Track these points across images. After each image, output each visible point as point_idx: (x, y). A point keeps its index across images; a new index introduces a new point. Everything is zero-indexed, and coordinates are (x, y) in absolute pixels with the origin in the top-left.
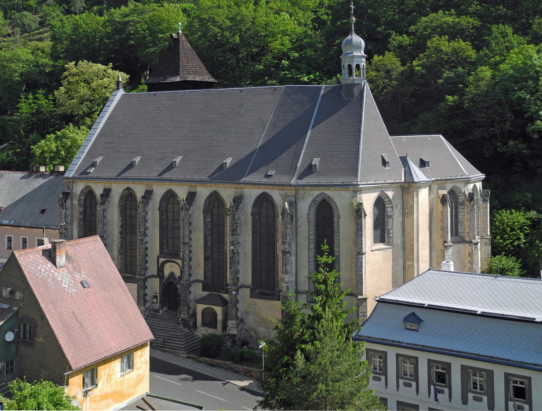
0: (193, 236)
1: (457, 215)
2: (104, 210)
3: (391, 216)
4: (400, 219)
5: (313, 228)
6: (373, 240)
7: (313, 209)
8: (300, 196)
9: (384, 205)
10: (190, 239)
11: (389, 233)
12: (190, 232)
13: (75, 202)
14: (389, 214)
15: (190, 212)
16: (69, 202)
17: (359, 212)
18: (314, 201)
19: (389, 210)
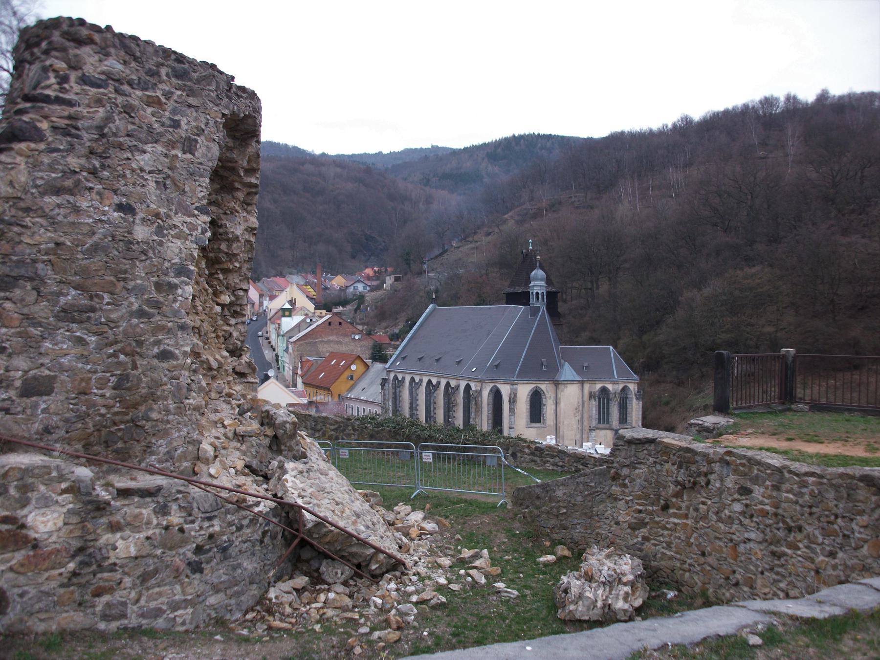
0: (435, 411)
1: (608, 409)
2: (400, 391)
3: (545, 405)
4: (554, 407)
5: (491, 410)
6: (529, 420)
7: (491, 396)
8: (484, 386)
9: (541, 396)
10: (435, 414)
11: (544, 417)
12: (435, 408)
13: (390, 385)
14: (544, 403)
15: (435, 395)
16: (386, 385)
17: (513, 400)
18: (491, 390)
19: (544, 400)
